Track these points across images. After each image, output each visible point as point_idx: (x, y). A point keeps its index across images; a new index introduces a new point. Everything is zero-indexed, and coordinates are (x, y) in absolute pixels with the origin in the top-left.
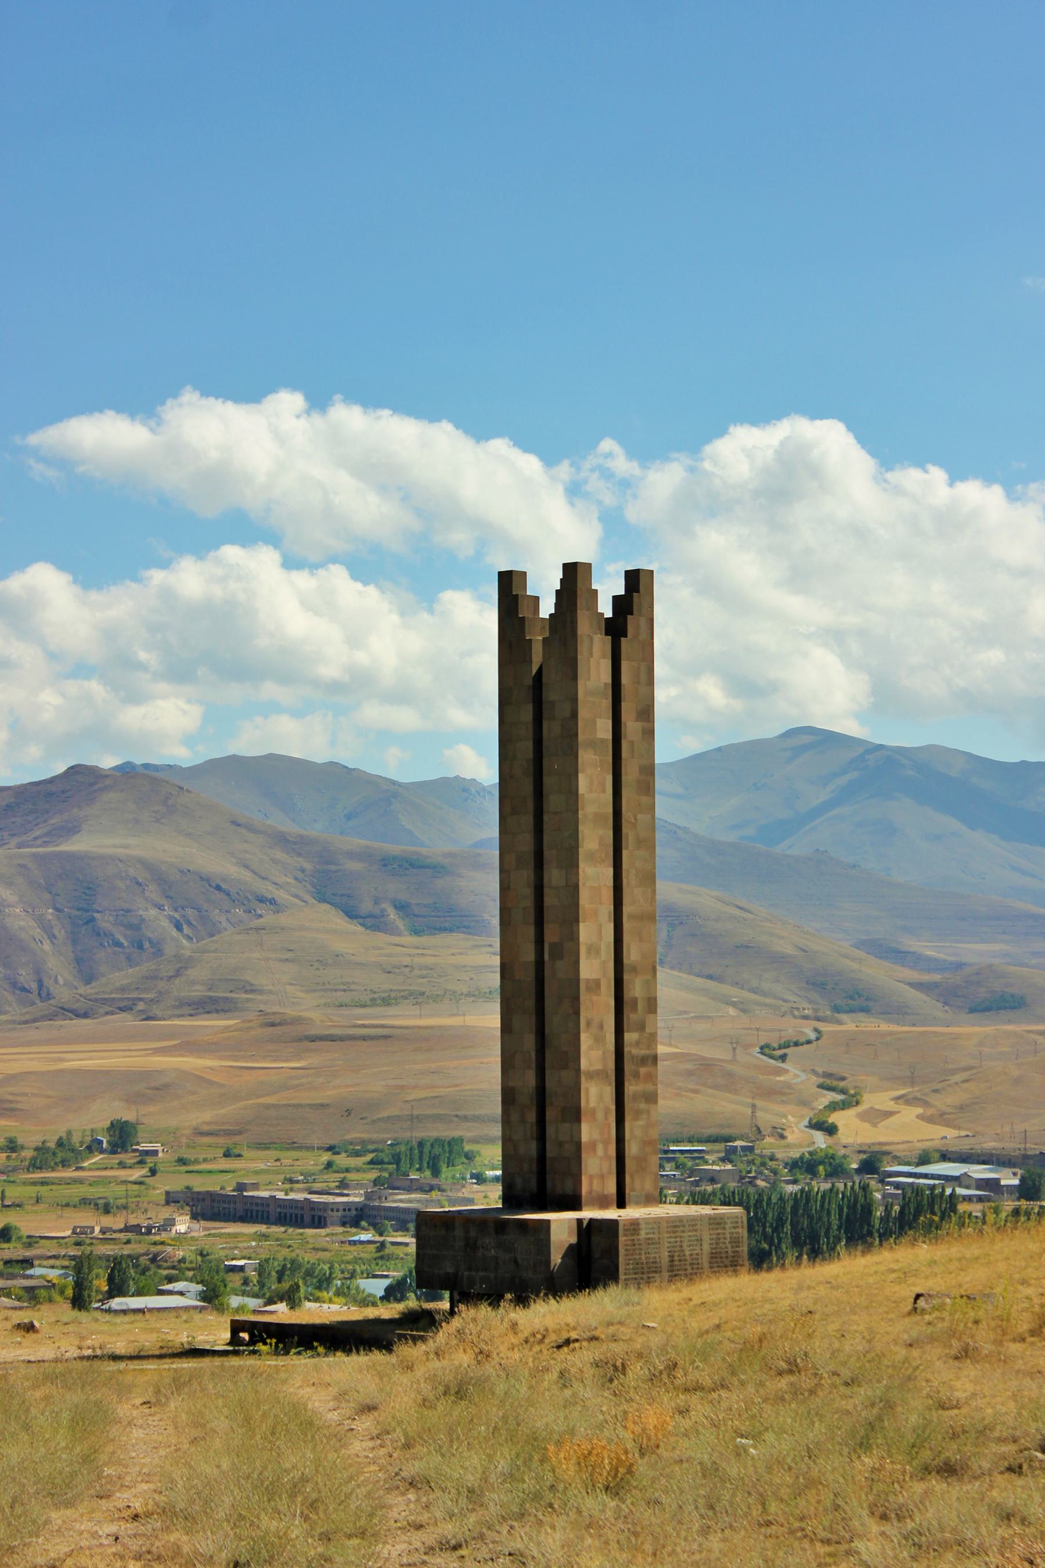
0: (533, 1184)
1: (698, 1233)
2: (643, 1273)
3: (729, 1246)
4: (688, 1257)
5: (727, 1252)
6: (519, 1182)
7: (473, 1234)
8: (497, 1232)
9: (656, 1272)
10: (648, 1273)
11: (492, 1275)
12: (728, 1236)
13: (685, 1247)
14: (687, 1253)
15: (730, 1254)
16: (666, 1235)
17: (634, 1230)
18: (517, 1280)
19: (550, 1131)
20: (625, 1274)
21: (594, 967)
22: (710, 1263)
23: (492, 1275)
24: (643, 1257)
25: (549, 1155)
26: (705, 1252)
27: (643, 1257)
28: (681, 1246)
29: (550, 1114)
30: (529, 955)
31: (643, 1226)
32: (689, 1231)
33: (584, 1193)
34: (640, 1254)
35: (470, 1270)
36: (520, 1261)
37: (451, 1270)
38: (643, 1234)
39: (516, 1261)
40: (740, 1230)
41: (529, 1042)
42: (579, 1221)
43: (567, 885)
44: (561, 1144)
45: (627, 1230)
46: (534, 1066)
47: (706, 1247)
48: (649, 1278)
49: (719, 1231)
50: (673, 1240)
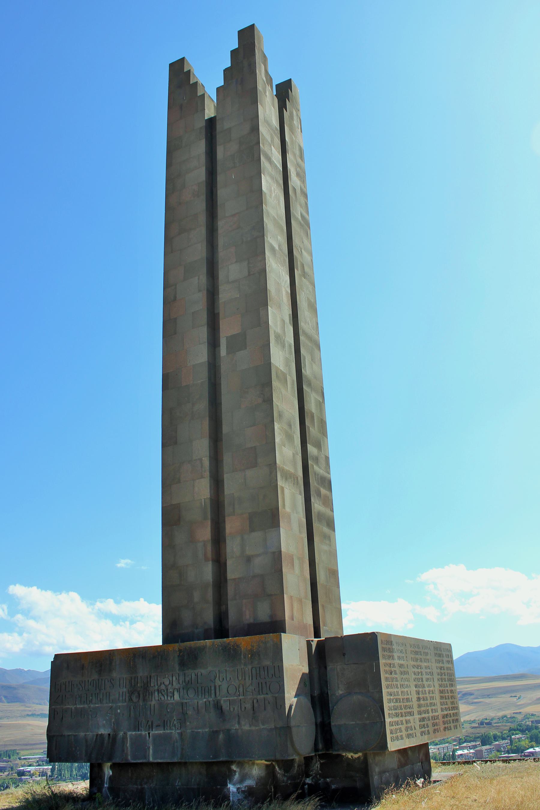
0: (208, 617)
6: (187, 617)
7: (142, 673)
8: (183, 664)
11: (175, 733)
18: (221, 736)
19: (233, 547)
21: (280, 358)
23: (175, 733)
25: (231, 575)
29: (231, 525)
30: (200, 355)
33: (286, 619)
35: (137, 728)
36: (225, 706)
37: (104, 731)
39: (218, 707)
41: (201, 448)
42: (320, 638)
43: (249, 275)
44: (249, 559)
46: (207, 474)
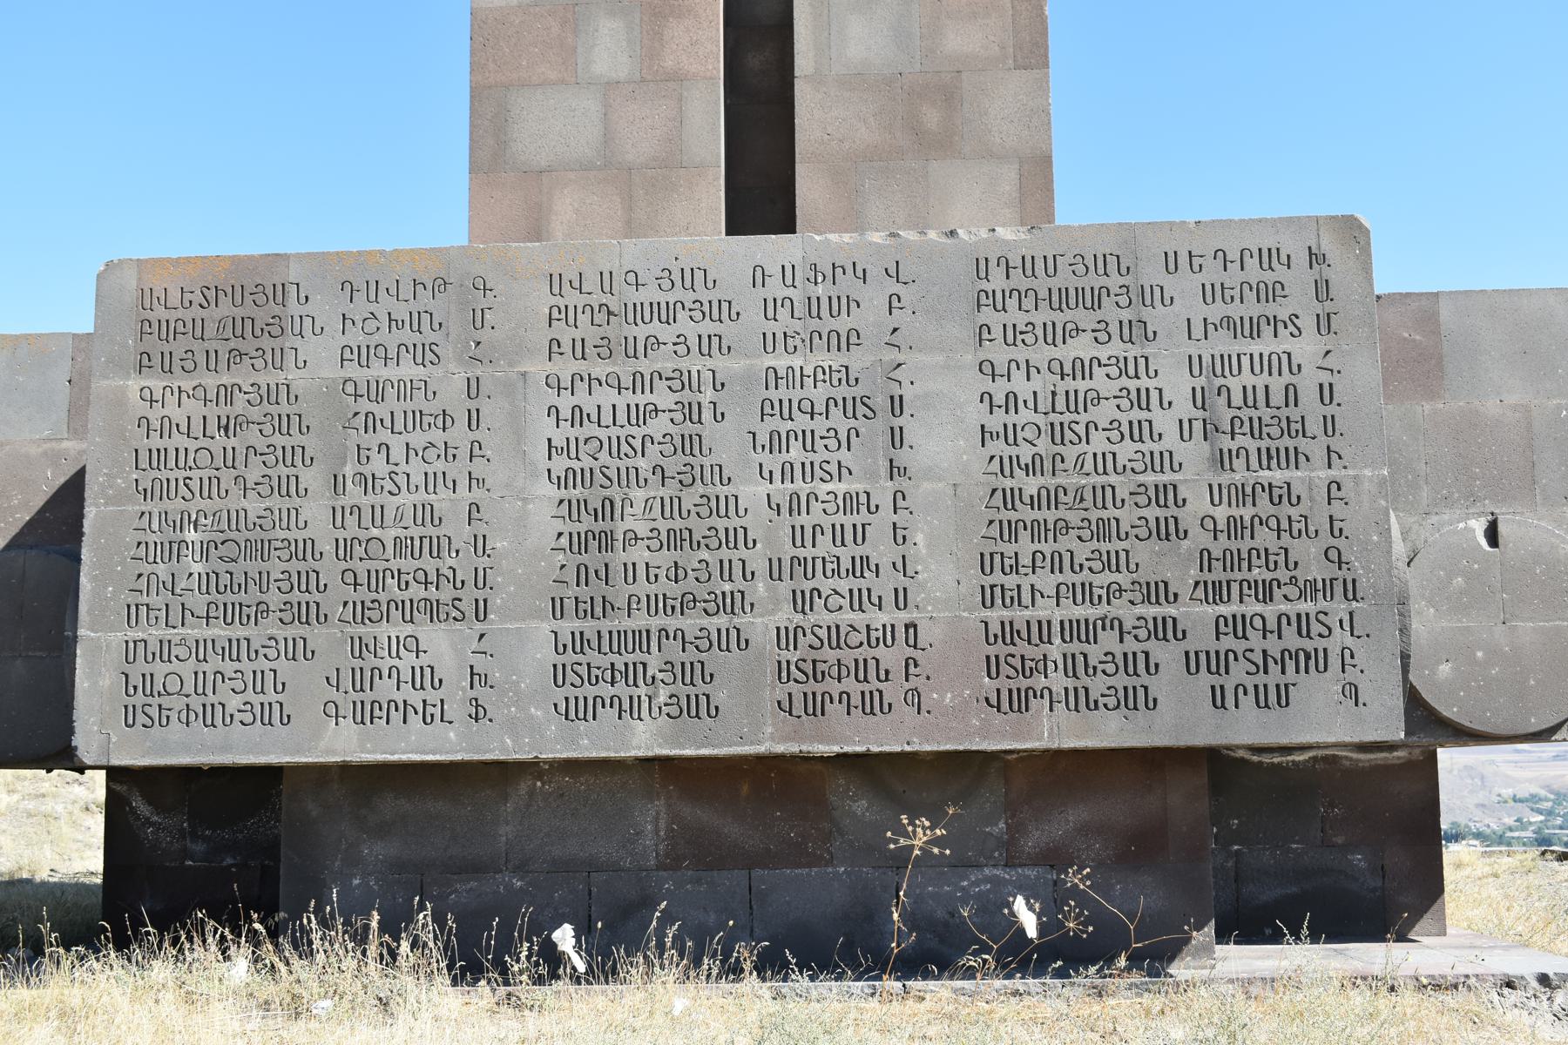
1: (858, 360)
2: (305, 615)
3: (1193, 453)
4: (757, 520)
5: (1166, 494)
9: (433, 610)
10: (363, 613)
12: (1177, 384)
13: (725, 442)
14: (752, 492)
15: (1198, 502)
16: (538, 367)
17: (239, 327)
20: (132, 614)
22: (986, 563)
24: (315, 511)
26: (921, 491)
27: (315, 511)
28: (690, 444)
31: (326, 307)
32: (768, 343)
34: (288, 487)
38: (316, 362)
40: (1306, 348)
45: (170, 331)
47: (946, 444)
48: (361, 647)
49: (1081, 347)
50: (606, 397)
